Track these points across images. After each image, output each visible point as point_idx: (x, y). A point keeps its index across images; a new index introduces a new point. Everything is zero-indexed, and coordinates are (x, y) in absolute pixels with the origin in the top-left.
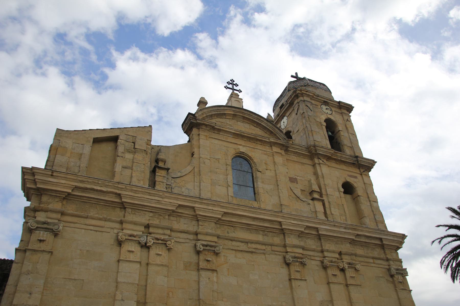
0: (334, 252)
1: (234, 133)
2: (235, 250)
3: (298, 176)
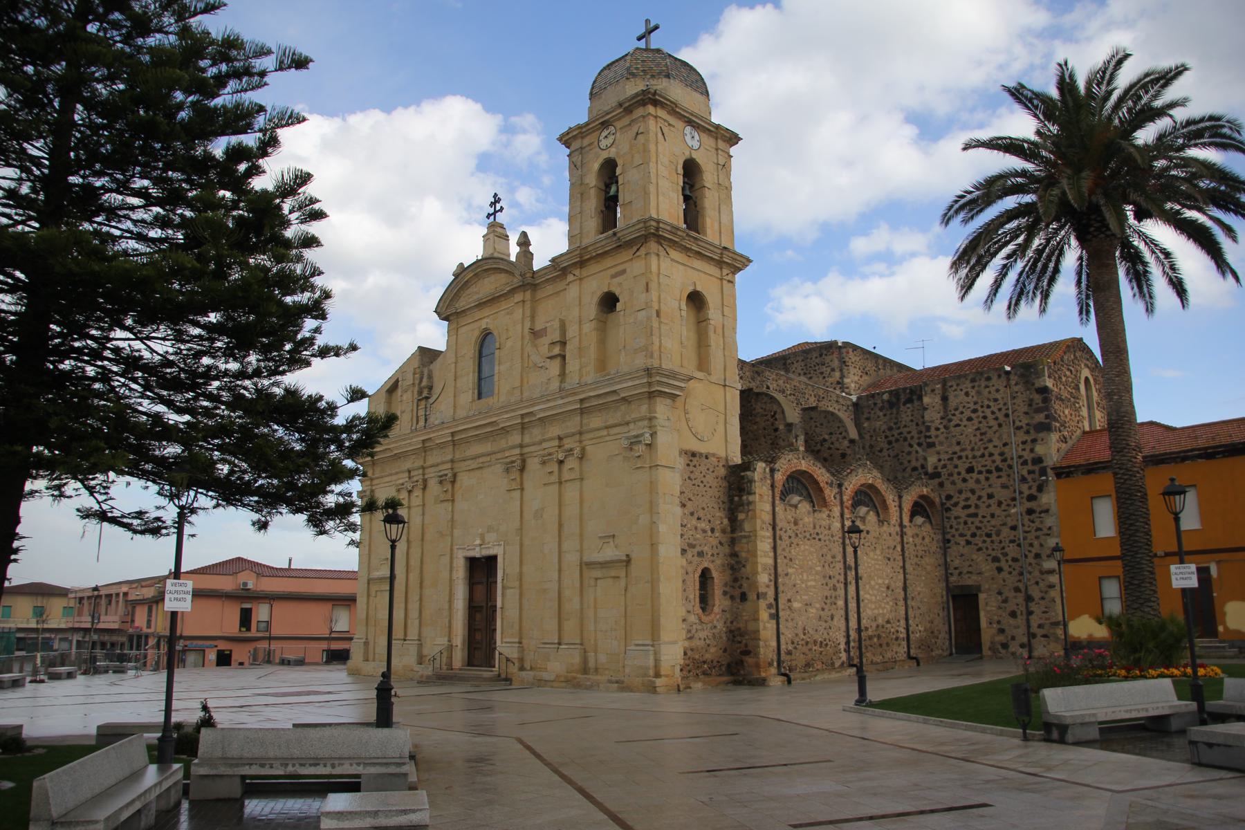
0: (551, 439)
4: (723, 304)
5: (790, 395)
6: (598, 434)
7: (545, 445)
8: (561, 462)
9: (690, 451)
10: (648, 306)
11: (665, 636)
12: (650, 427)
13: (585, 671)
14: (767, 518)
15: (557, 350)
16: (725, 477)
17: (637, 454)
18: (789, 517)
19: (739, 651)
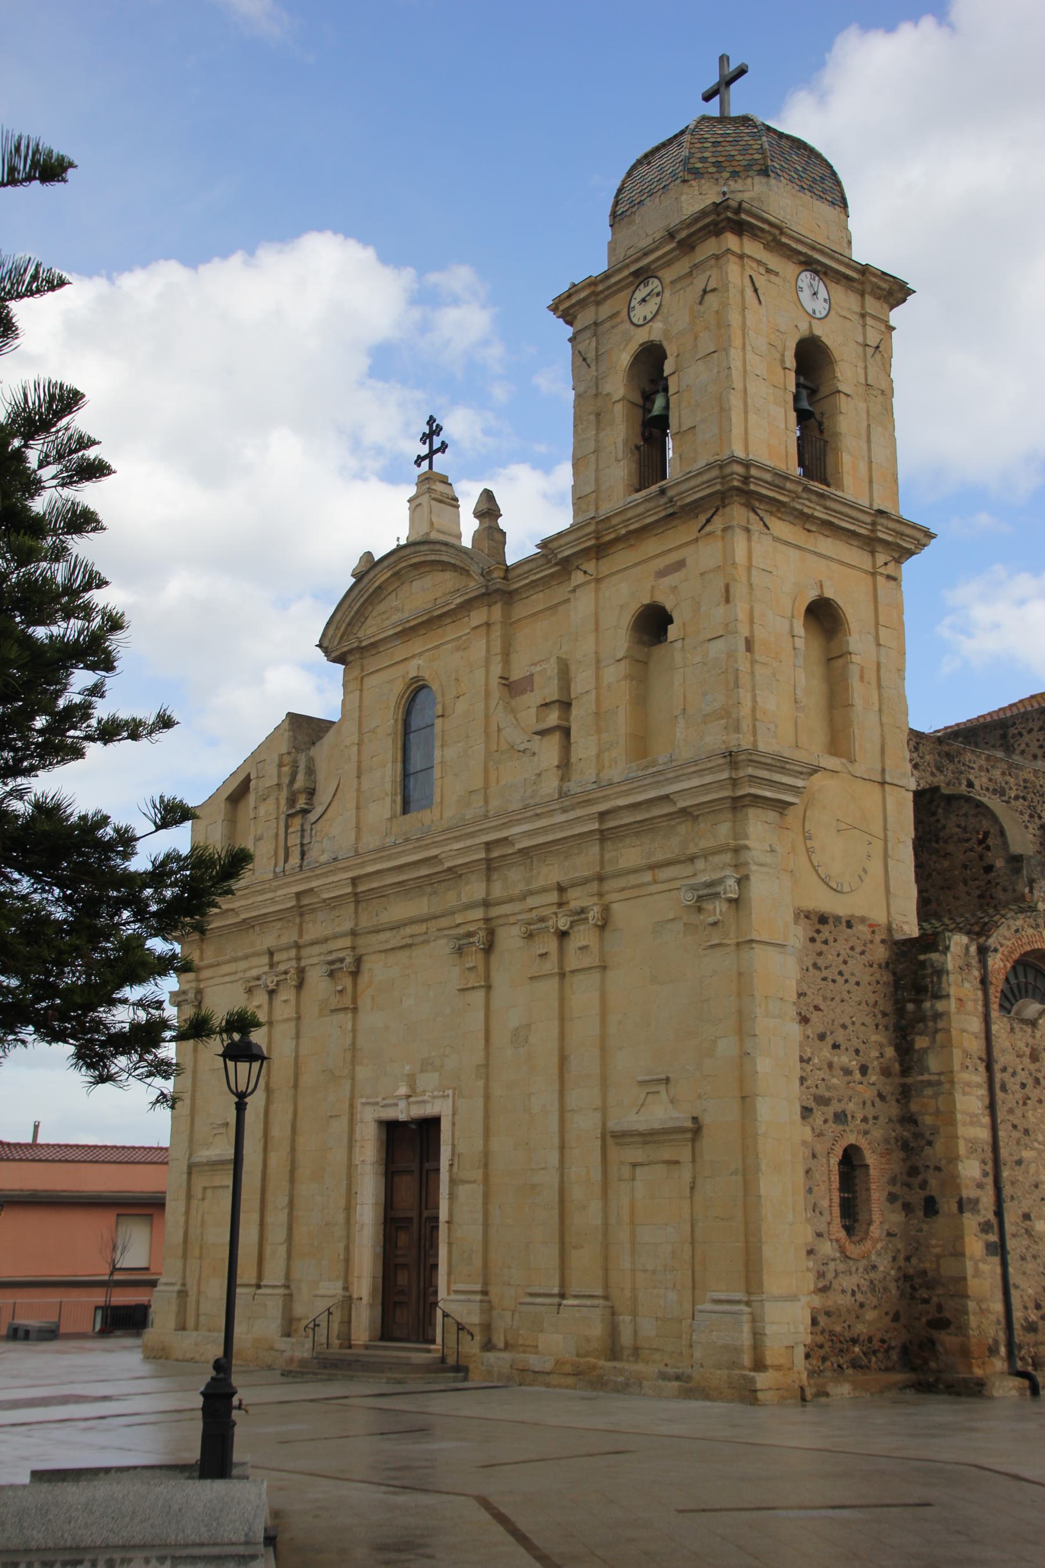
0: (544, 890)
1: (396, 634)
2: (385, 951)
3: (535, 664)
4: (877, 624)
5: (1017, 798)
6: (633, 880)
7: (531, 902)
8: (563, 935)
9: (816, 913)
10: (729, 629)
11: (773, 1284)
12: (736, 866)
13: (613, 1352)
14: (976, 1046)
15: (553, 718)
16: (887, 964)
17: (711, 920)
18: (1021, 1045)
19: (924, 1320)
